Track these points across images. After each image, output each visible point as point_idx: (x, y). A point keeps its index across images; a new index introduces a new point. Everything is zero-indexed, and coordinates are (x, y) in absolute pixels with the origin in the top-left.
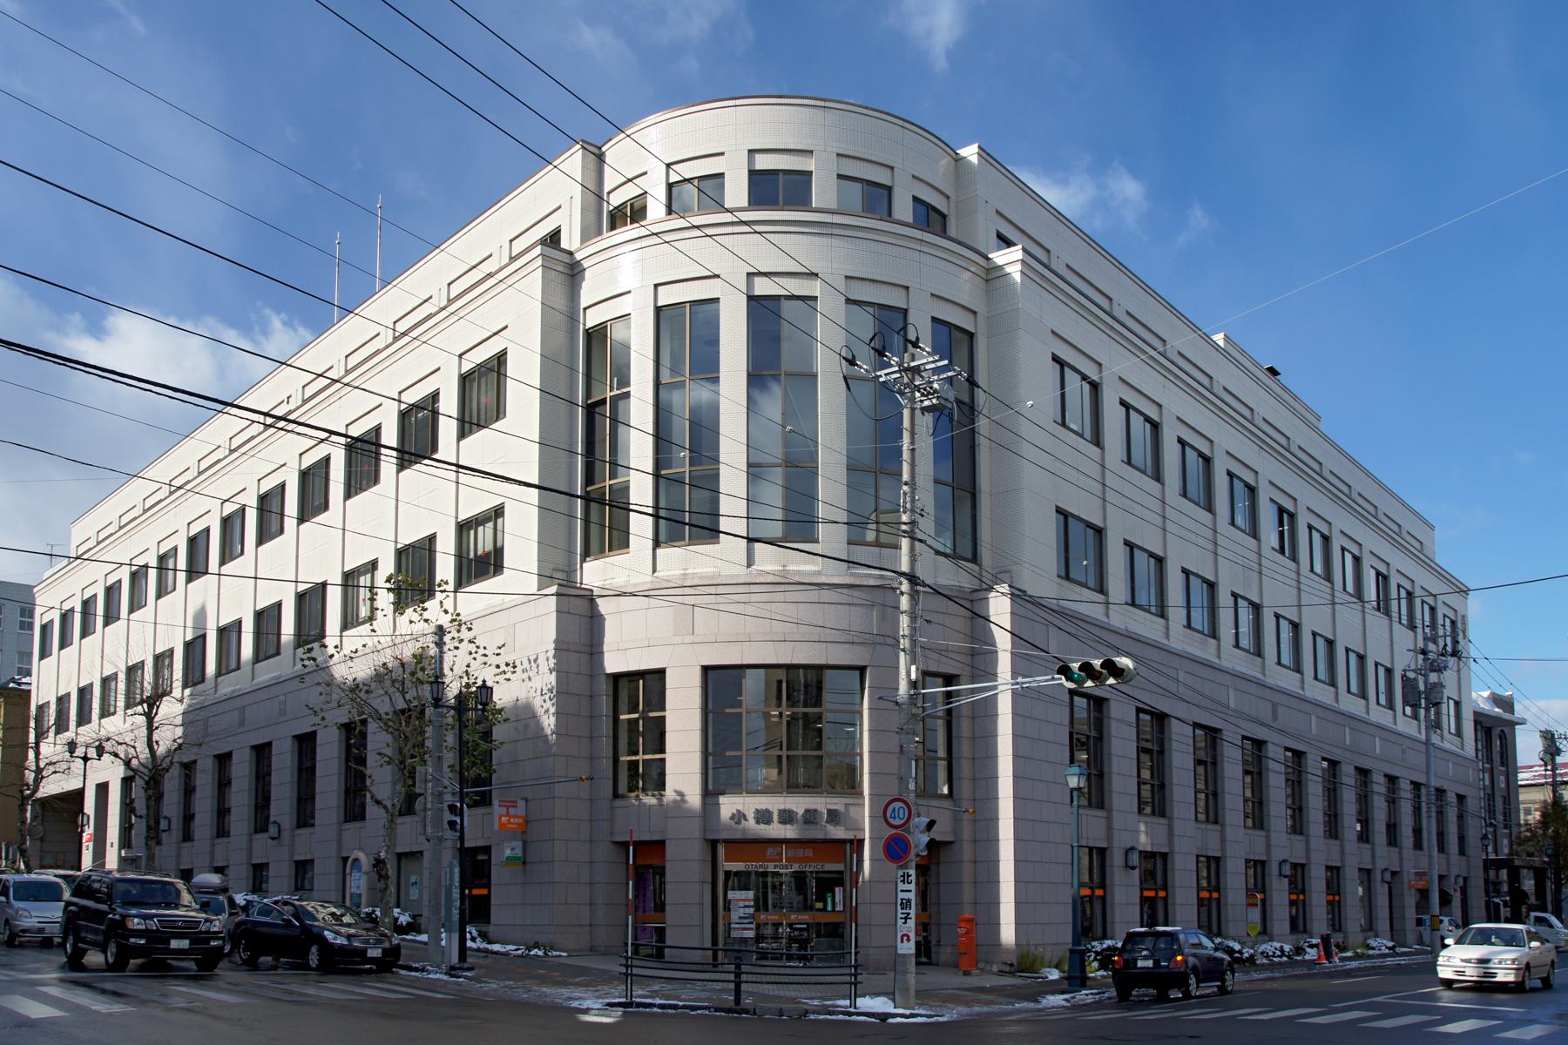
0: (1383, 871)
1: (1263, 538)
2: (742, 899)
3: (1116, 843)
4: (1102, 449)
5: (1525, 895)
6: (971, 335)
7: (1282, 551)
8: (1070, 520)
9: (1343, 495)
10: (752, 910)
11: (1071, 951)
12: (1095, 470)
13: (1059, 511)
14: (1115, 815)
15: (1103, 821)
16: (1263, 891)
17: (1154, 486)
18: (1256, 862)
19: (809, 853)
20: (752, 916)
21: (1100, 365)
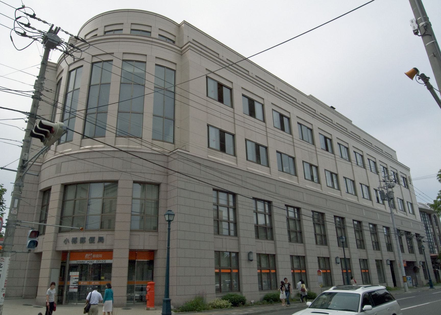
0: (337, 258)
1: (316, 145)
2: (75, 275)
3: (242, 250)
4: (234, 109)
5: (90, 257)
6: (175, 71)
7: (327, 150)
8: (282, 155)
9: (343, 130)
10: (78, 280)
11: (164, 301)
12: (264, 128)
13: (278, 152)
14: (277, 242)
15: (303, 247)
16: (330, 270)
17: (313, 147)
18: (298, 257)
19: (101, 256)
20: (77, 283)
21: (290, 113)
